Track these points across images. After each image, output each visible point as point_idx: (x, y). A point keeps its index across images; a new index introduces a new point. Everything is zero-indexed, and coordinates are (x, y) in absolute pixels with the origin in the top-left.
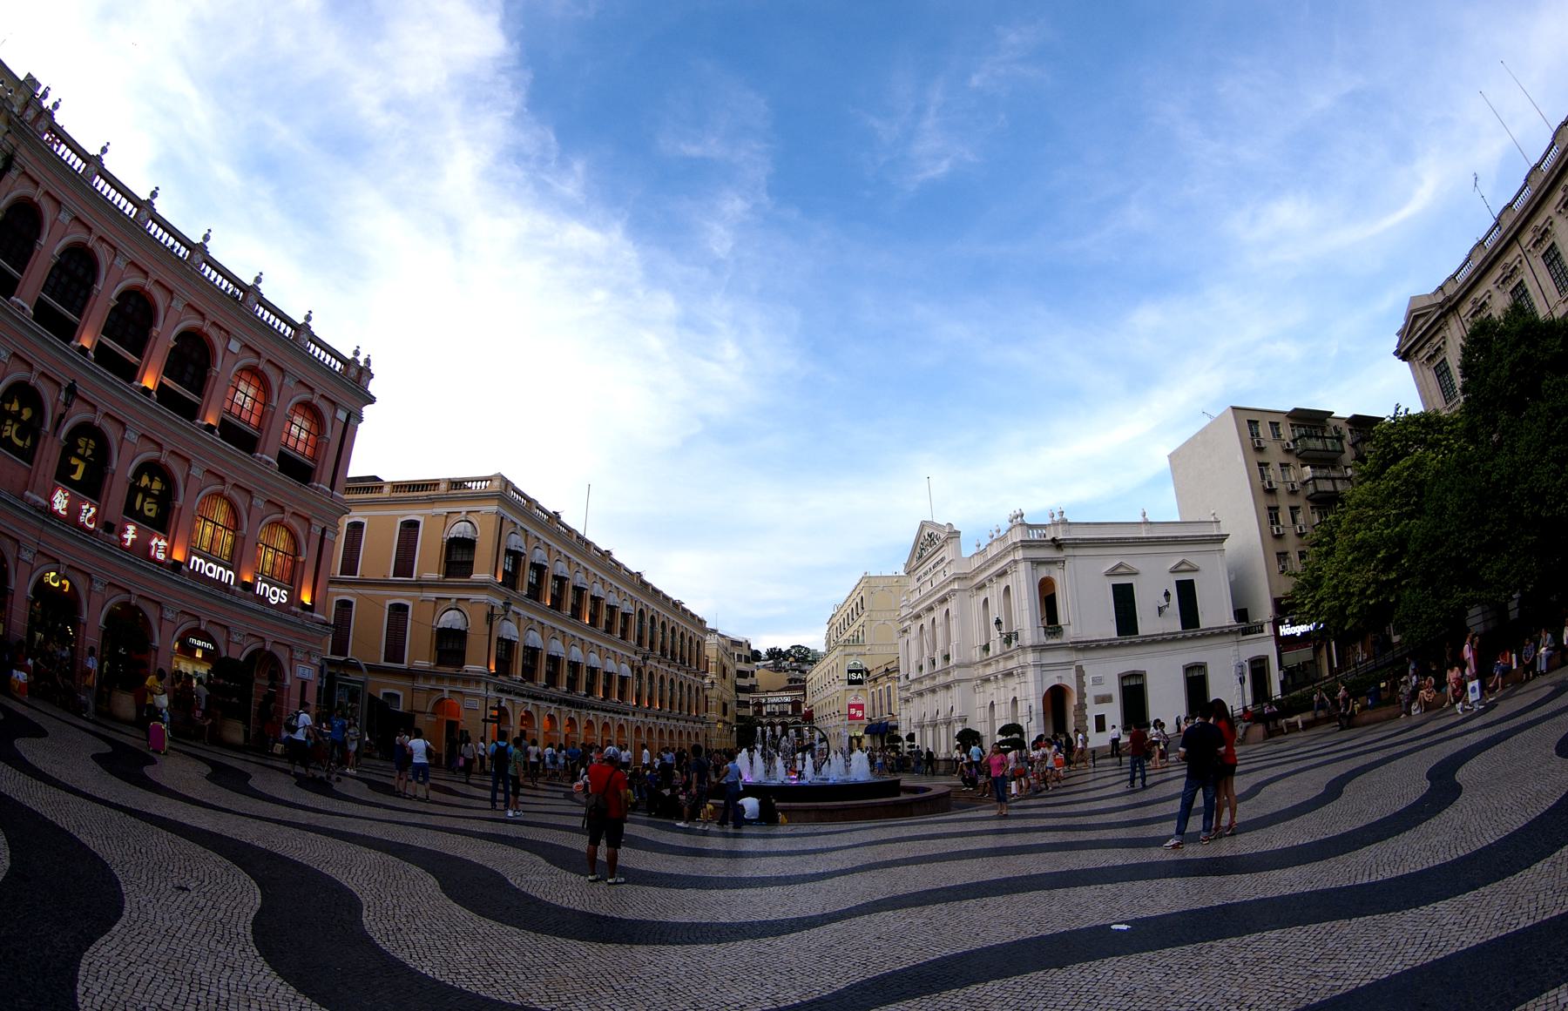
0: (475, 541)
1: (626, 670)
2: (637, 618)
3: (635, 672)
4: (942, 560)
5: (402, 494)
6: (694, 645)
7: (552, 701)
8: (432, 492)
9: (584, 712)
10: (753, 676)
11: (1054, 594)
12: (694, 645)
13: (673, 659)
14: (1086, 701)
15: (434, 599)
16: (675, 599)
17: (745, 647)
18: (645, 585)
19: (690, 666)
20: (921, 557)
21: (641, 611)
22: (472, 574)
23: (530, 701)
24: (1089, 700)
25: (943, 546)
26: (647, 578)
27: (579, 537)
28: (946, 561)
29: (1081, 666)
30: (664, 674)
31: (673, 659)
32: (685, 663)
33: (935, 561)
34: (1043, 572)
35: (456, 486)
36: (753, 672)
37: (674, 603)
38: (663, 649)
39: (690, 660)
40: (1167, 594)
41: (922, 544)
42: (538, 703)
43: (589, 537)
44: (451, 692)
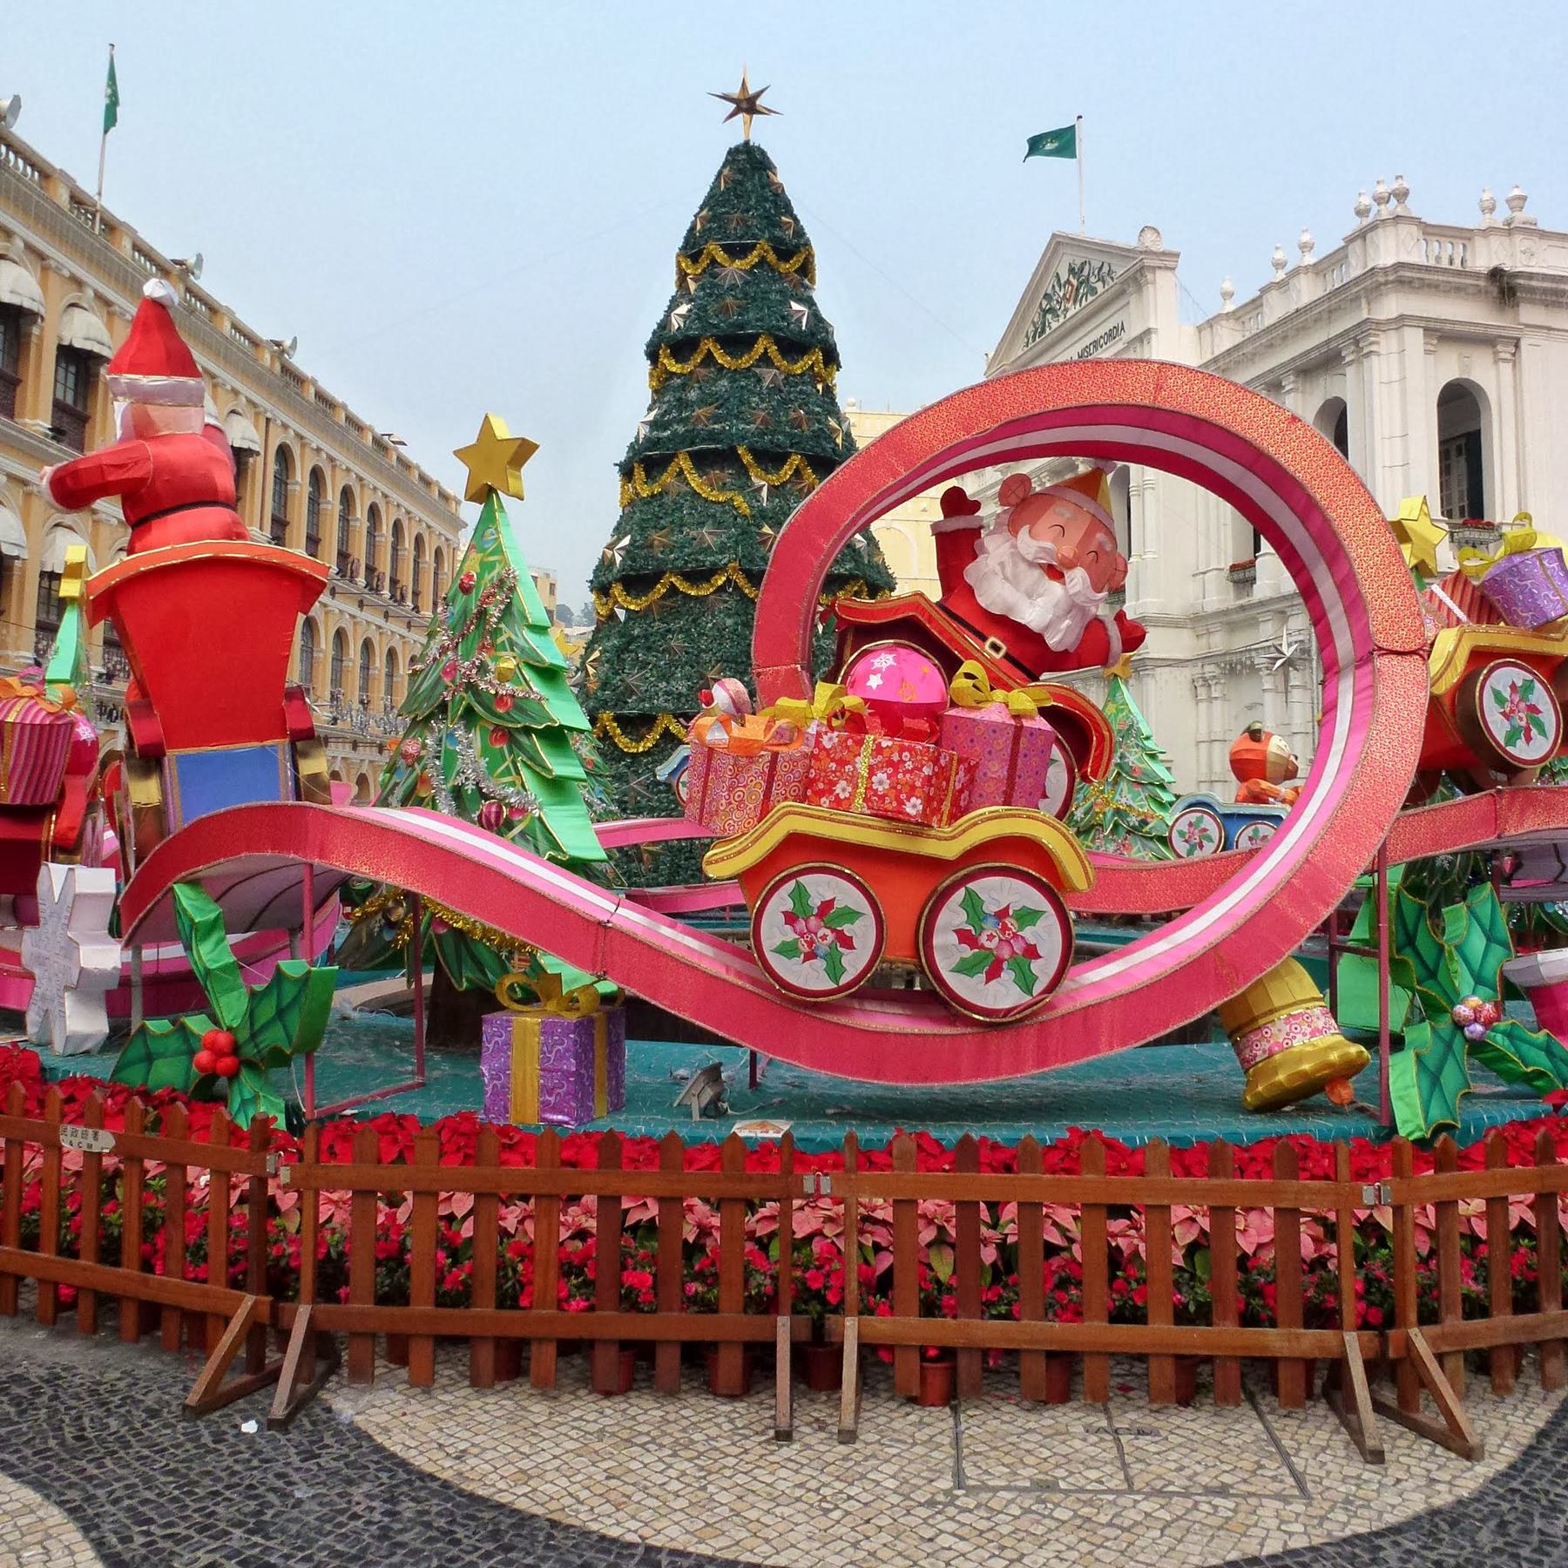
2: (272, 467)
4: (1112, 335)
6: (429, 557)
11: (1478, 432)
12: (429, 557)
13: (373, 587)
16: (379, 431)
18: (294, 377)
19: (416, 608)
20: (1041, 330)
21: (284, 454)
25: (1121, 293)
26: (299, 361)
27: (78, 200)
28: (1126, 336)
30: (347, 625)
31: (373, 587)
32: (403, 598)
33: (1087, 341)
34: (1450, 367)
37: (377, 442)
38: (343, 556)
39: (416, 594)
41: (1047, 296)
43: (115, 204)
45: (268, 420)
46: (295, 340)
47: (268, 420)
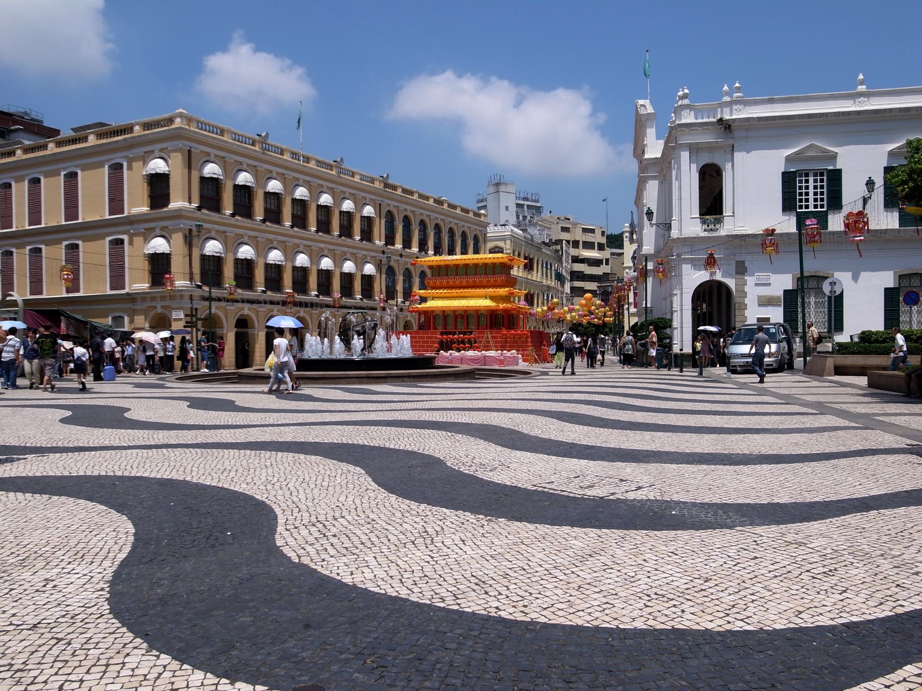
0: (168, 175)
1: (369, 269)
3: (384, 270)
5: (104, 141)
7: (272, 303)
8: (129, 136)
9: (315, 311)
10: (607, 264)
14: (747, 301)
15: (143, 230)
17: (598, 233)
22: (169, 203)
23: (247, 306)
24: (751, 301)
29: (743, 262)
34: (706, 159)
35: (148, 127)
36: (607, 260)
40: (870, 184)
42: (255, 306)
44: (163, 307)
45: (380, 204)
46: (388, 174)
47: (380, 204)
